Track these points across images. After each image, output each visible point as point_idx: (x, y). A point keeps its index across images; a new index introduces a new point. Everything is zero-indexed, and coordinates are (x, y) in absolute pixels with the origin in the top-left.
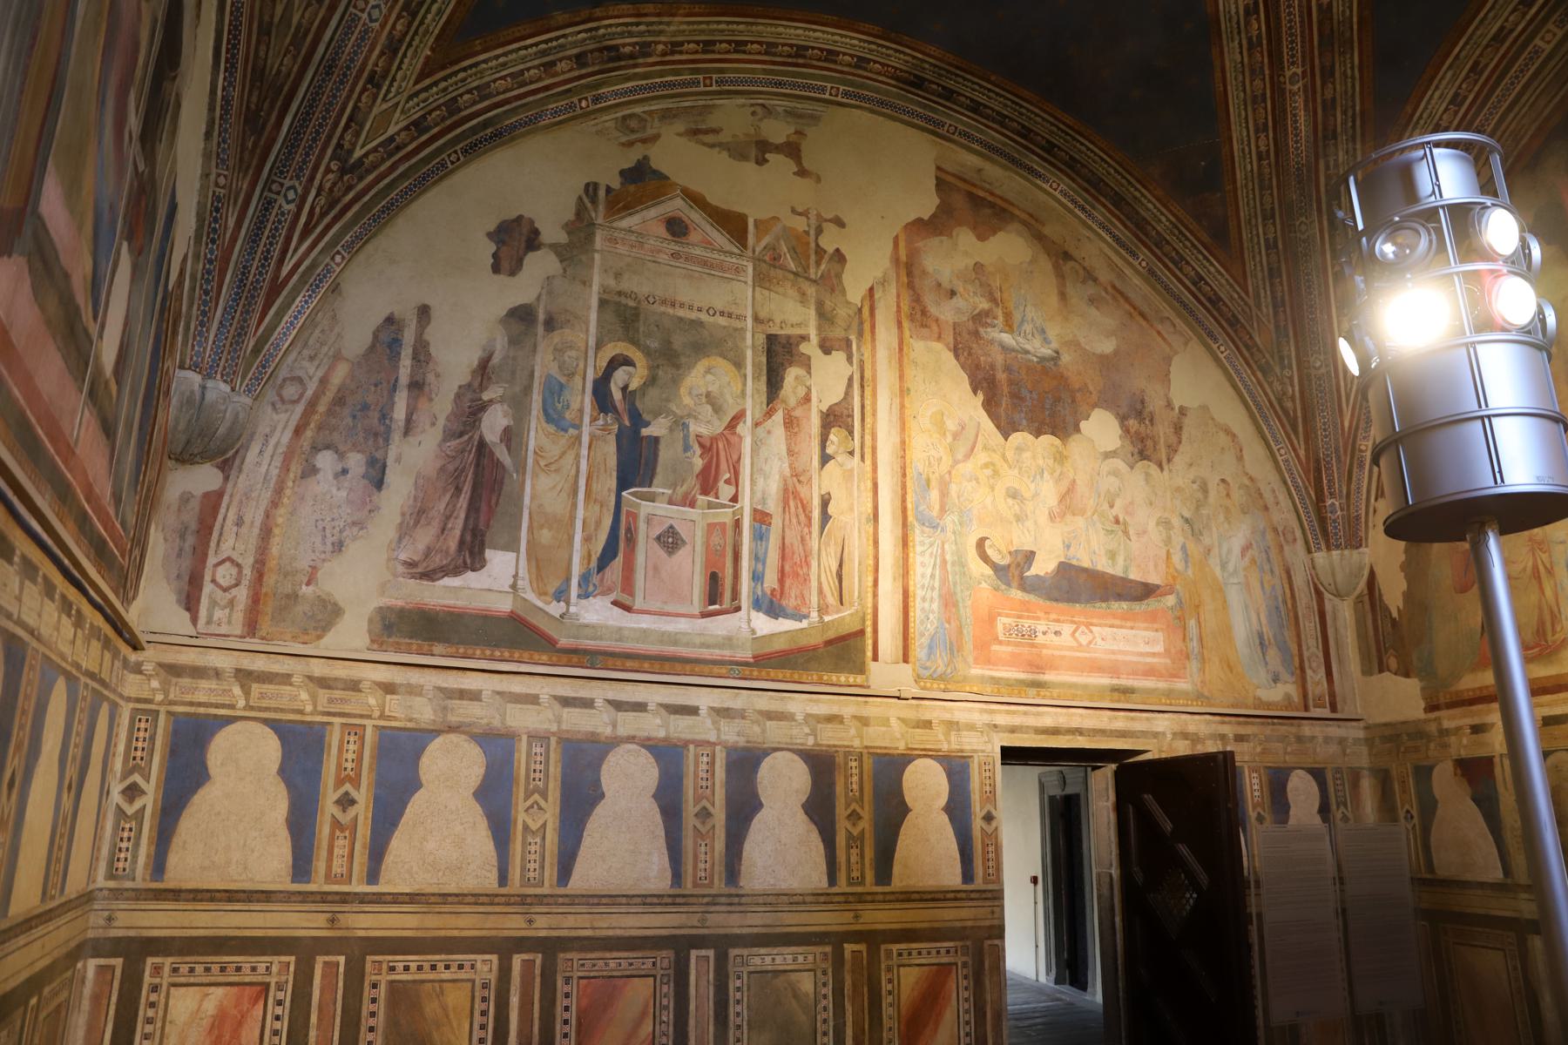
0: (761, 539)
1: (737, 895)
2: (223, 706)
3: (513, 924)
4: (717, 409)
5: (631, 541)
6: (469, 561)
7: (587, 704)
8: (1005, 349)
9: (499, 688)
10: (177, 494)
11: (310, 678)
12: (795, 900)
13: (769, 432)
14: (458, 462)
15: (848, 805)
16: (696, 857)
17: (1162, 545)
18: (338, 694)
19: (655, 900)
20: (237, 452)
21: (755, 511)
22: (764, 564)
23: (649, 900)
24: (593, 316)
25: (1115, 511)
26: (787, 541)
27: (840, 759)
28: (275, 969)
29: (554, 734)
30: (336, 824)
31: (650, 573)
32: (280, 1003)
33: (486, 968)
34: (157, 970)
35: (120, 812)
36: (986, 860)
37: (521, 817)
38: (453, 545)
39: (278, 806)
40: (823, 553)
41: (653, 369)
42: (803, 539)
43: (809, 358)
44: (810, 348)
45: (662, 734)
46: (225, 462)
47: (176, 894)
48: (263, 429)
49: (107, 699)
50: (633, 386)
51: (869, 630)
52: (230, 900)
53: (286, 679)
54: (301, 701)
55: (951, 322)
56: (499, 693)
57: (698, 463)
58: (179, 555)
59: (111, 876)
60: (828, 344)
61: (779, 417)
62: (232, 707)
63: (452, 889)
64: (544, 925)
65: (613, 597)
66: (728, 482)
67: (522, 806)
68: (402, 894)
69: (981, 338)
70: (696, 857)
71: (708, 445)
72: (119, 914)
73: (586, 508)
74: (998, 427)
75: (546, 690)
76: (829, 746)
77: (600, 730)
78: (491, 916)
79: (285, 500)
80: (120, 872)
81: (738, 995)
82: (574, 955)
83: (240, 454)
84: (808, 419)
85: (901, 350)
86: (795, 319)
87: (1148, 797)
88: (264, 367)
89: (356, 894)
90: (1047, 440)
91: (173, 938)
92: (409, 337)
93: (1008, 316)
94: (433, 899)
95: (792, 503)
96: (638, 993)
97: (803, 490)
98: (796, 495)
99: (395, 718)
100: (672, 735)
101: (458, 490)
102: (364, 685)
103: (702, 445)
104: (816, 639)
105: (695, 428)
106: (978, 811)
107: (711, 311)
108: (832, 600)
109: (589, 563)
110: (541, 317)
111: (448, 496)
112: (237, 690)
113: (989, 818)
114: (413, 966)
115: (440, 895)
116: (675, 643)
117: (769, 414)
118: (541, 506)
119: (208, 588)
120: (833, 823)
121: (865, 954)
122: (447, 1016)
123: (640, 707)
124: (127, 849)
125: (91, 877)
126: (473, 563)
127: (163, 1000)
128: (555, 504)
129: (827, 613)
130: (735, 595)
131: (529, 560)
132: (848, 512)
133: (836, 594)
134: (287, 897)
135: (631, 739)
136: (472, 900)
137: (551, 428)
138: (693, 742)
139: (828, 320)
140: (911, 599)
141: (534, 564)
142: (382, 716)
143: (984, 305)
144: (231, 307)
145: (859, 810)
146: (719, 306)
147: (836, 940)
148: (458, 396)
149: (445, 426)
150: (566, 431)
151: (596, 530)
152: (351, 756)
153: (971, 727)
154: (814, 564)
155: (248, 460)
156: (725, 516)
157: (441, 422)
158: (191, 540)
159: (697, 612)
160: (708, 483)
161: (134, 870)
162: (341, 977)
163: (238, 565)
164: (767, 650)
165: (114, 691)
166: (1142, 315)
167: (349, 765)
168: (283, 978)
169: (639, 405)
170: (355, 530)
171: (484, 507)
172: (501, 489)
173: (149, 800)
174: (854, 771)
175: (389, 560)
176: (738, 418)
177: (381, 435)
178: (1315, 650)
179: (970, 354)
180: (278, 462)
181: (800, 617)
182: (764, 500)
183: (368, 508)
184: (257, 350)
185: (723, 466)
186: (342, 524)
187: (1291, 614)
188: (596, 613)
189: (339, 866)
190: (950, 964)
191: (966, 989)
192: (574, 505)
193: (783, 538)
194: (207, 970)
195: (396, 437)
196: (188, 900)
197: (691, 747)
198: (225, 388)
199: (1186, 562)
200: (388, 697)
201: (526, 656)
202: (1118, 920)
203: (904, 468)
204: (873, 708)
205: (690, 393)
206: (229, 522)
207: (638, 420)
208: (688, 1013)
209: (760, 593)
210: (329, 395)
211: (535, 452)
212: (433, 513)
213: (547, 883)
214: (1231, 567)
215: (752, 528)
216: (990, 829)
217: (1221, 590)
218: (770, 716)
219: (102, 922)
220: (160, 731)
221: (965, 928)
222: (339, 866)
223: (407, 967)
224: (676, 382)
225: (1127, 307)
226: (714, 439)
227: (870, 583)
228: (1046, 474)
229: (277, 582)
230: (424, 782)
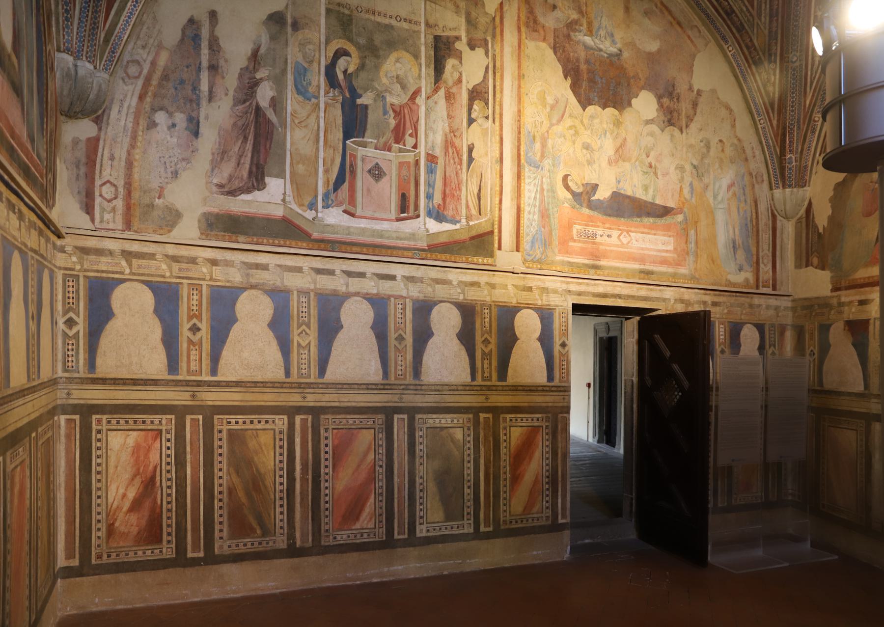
0: (432, 173)
1: (420, 385)
2: (117, 273)
3: (294, 399)
4: (403, 87)
5: (353, 172)
7: (331, 273)
8: (587, 47)
9: (278, 263)
10: (70, 139)
11: (167, 256)
12: (453, 389)
13: (436, 103)
14: (244, 119)
15: (482, 335)
16: (396, 363)
17: (678, 182)
18: (184, 266)
19: (374, 387)
20: (104, 111)
21: (428, 154)
22: (433, 189)
23: (370, 387)
24: (323, 21)
25: (649, 160)
26: (447, 174)
27: (478, 308)
28: (164, 422)
29: (312, 290)
30: (190, 342)
31: (365, 193)
32: (169, 440)
33: (281, 423)
34: (99, 422)
35: (65, 335)
36: (561, 369)
37: (296, 339)
38: (245, 174)
39: (157, 332)
40: (469, 183)
41: (363, 58)
42: (457, 173)
43: (461, 52)
44: (462, 46)
45: (375, 291)
46: (98, 118)
47: (104, 381)
48: (118, 96)
49: (47, 267)
50: (350, 70)
51: (496, 231)
52: (134, 384)
53: (152, 256)
54: (163, 270)
55: (552, 28)
56: (279, 266)
57: (393, 123)
58: (77, 178)
59: (65, 370)
60: (473, 43)
61: (442, 92)
62: (122, 273)
63: (259, 378)
64: (312, 399)
65: (343, 207)
66: (411, 135)
67: (296, 332)
68: (231, 382)
69: (572, 40)
70: (396, 363)
71: (398, 110)
72: (73, 391)
73: (325, 151)
74: (579, 101)
75: (306, 264)
76: (472, 300)
77: (339, 288)
78: (282, 394)
79: (139, 144)
80: (70, 368)
81: (421, 440)
82: (330, 416)
83: (107, 111)
84: (461, 94)
85: (519, 47)
86: (451, 25)
87: (657, 337)
88: (113, 52)
89: (205, 381)
90: (610, 111)
91: (106, 405)
92: (205, 33)
93: (590, 24)
94: (249, 385)
96: (366, 437)
97: (457, 142)
98: (453, 144)
99: (219, 281)
100: (381, 292)
101: (246, 139)
102: (199, 260)
103: (394, 111)
104: (465, 236)
105: (390, 99)
106: (557, 341)
107: (398, 18)
108: (474, 212)
109: (328, 186)
110: (289, 20)
111: (240, 142)
112: (124, 263)
113: (563, 345)
114: (240, 421)
115: (253, 382)
116: (381, 237)
117: (436, 90)
118: (297, 149)
119: (98, 200)
120: (474, 345)
121: (491, 419)
122: (261, 448)
123: (362, 275)
124: (72, 356)
125: (54, 371)
126: (258, 185)
127: (104, 438)
128: (306, 149)
129: (472, 220)
130: (417, 207)
132: (485, 156)
133: (477, 208)
134: (167, 383)
135: (357, 294)
136: (271, 385)
137: (301, 98)
138: (393, 296)
139: (473, 25)
140: (522, 212)
141: (295, 186)
142: (211, 279)
143: (574, 16)
144: (85, 8)
145: (489, 338)
146: (403, 14)
147: (475, 411)
148: (241, 76)
149: (234, 96)
151: (331, 165)
152: (195, 302)
153: (555, 291)
154: (464, 189)
155: (112, 117)
156: (409, 157)
157: (231, 93)
158: (83, 170)
159: (394, 217)
160: (399, 137)
161: (78, 367)
162: (201, 427)
163: (115, 186)
164: (435, 242)
165: (50, 262)
166: (679, 24)
167: (195, 308)
168: (169, 427)
170: (184, 163)
173: (81, 327)
174: (486, 315)
175: (207, 183)
176: (417, 93)
177: (194, 101)
178: (767, 252)
179: (564, 51)
180: (131, 118)
181: (455, 222)
182: (433, 148)
183: (191, 149)
184: (107, 40)
185: (408, 124)
186: (176, 160)
187: (755, 229)
188: (334, 217)
189: (194, 366)
190: (540, 426)
191: (547, 440)
192: (317, 149)
194: (127, 422)
195: (204, 103)
196: (111, 384)
197: (392, 299)
198: (90, 66)
199: (692, 194)
200: (214, 268)
201: (293, 243)
202: (635, 406)
203: (519, 128)
204: (498, 279)
205: (386, 75)
207: (355, 94)
208: (393, 449)
209: (431, 207)
210: (158, 74)
212: (231, 153)
213: (312, 376)
214: (720, 198)
215: (426, 166)
216: (564, 352)
217: (712, 212)
218: (437, 281)
219: (65, 396)
220: (81, 287)
221: (547, 407)
222: (194, 366)
223: (237, 422)
224: (377, 67)
225: (670, 18)
226: (402, 107)
227: (497, 202)
228: (608, 133)
229: (140, 197)
230: (239, 318)
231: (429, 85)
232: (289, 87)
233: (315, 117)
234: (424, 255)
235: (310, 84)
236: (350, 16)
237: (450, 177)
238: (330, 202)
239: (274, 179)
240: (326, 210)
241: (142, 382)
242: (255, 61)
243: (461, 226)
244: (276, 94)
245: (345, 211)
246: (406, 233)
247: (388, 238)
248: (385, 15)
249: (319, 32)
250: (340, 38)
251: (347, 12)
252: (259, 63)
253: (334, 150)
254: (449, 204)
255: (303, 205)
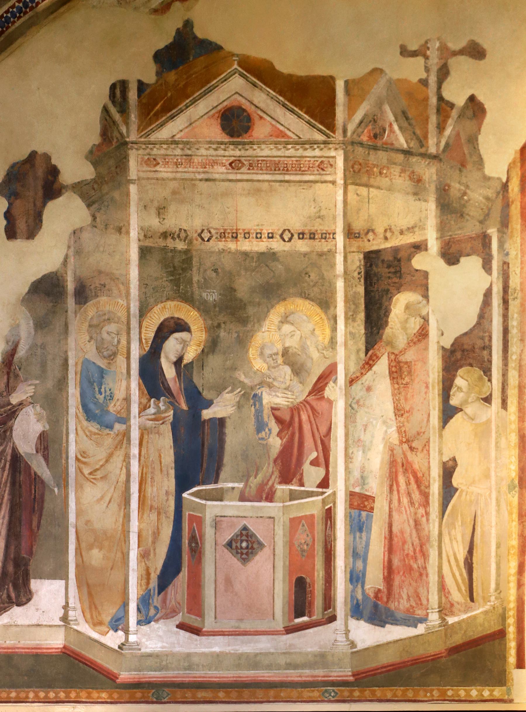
0: (361, 530)
6: (13, 595)
21: (352, 495)
22: (365, 561)
31: (221, 587)
40: (446, 539)
42: (417, 523)
66: (315, 463)
71: (287, 418)
73: (140, 518)
84: (424, 361)
95: (402, 480)
98: (407, 467)
103: (279, 420)
109: (148, 583)
118: (88, 522)
126: (18, 596)
131: (79, 587)
137: (93, 427)
141: (85, 590)
150: (111, 427)
151: (154, 542)
154: (433, 554)
169: (197, 380)
171: (25, 532)
172: (41, 509)
185: (309, 442)
192: (127, 517)
193: (390, 526)
205: (262, 354)
209: (360, 596)
211: (77, 459)
215: (349, 517)
226: (295, 410)
231: (353, 357)
232: (72, 411)
233: (121, 458)
234: (346, 694)
235: (111, 397)
236: (187, 252)
237: (402, 532)
238: (152, 612)
239: (47, 582)
240: (145, 628)
242: (8, 374)
243: (427, 628)
244: (47, 427)
245: (181, 626)
246: (307, 654)
247: (269, 667)
248: (259, 236)
249: (128, 294)
250: (168, 299)
251: (181, 246)
252: (17, 376)
253: (159, 514)
254: (401, 587)
255: (101, 623)
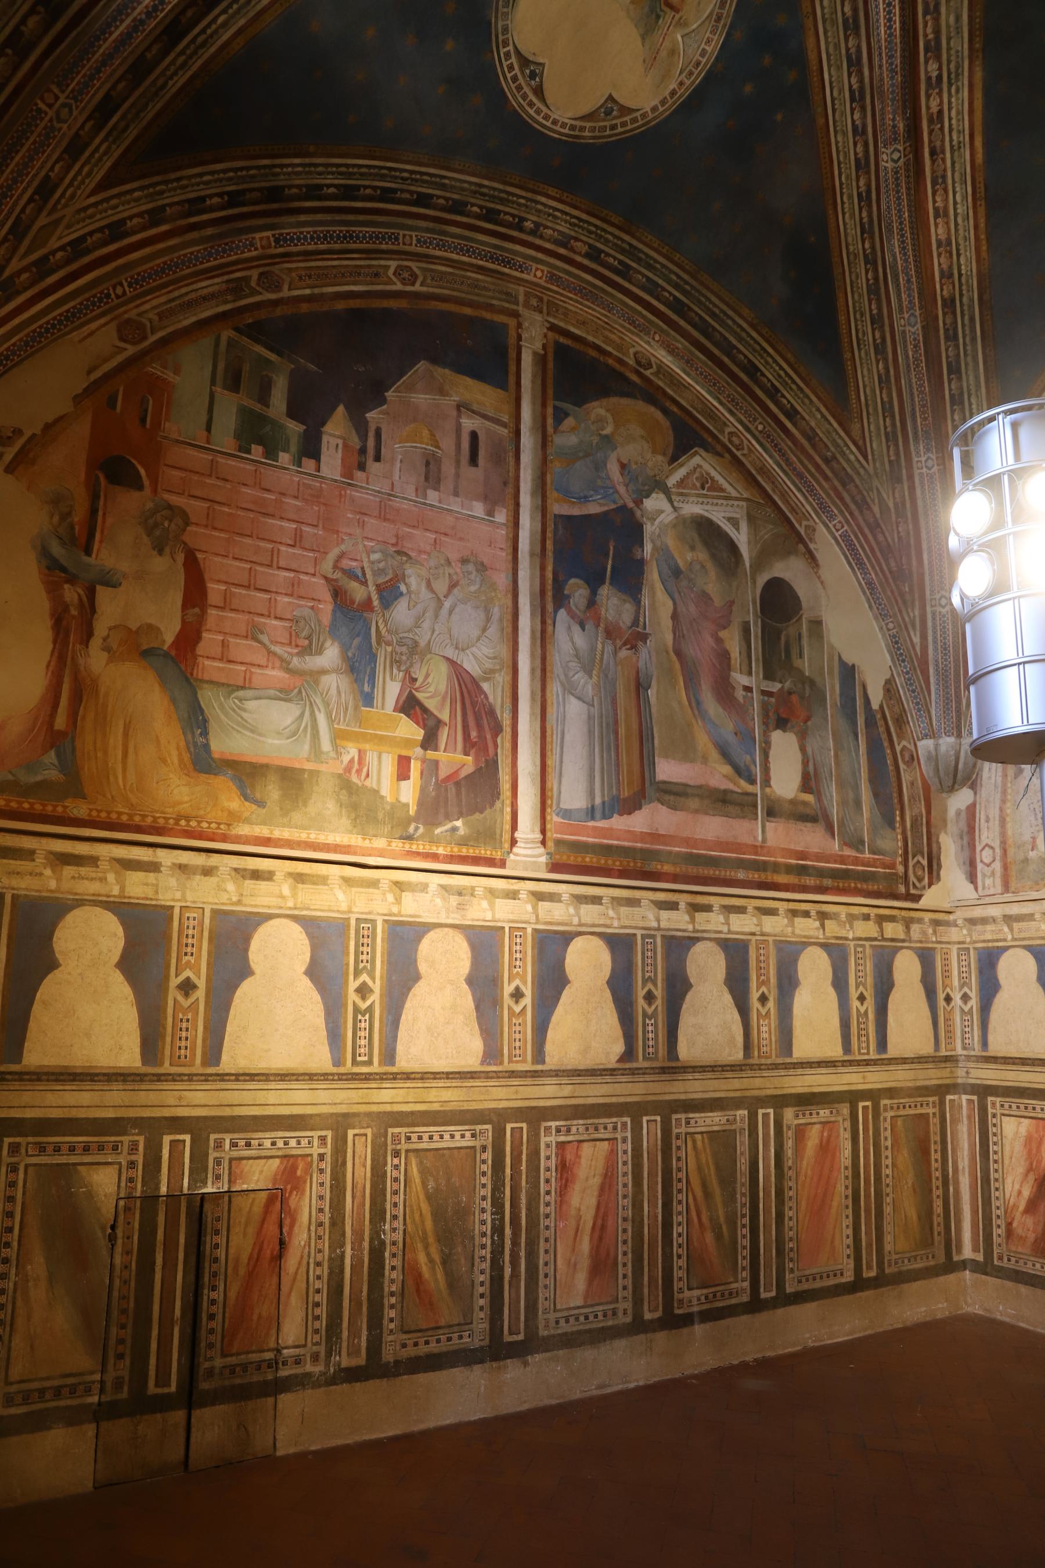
52: (1023, 1064)
59: (964, 1048)
62: (1005, 940)
79: (1009, 797)
112: (1006, 929)
163: (992, 848)
173: (974, 1003)
206: (983, 821)
219: (964, 1074)
241: (1030, 1062)
